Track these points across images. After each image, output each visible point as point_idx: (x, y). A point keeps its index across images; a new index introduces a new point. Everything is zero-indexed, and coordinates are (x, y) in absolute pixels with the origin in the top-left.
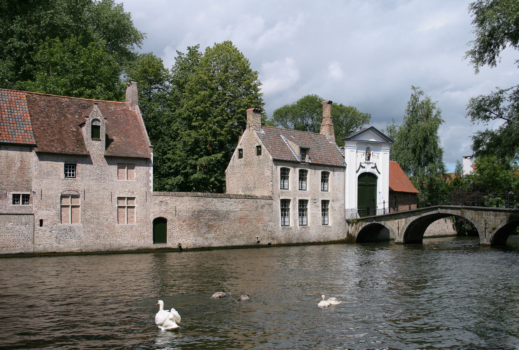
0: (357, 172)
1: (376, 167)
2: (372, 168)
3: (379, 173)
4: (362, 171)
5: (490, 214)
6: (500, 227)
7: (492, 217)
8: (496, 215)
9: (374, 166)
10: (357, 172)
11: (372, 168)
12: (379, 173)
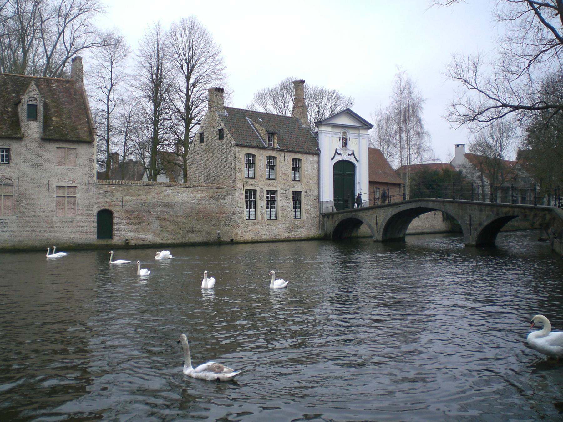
0: (332, 159)
1: (353, 154)
2: (349, 155)
3: (358, 161)
4: (338, 158)
5: (475, 209)
6: (485, 224)
7: (477, 212)
8: (481, 211)
9: (351, 153)
10: (332, 159)
11: (349, 155)
12: (358, 161)
